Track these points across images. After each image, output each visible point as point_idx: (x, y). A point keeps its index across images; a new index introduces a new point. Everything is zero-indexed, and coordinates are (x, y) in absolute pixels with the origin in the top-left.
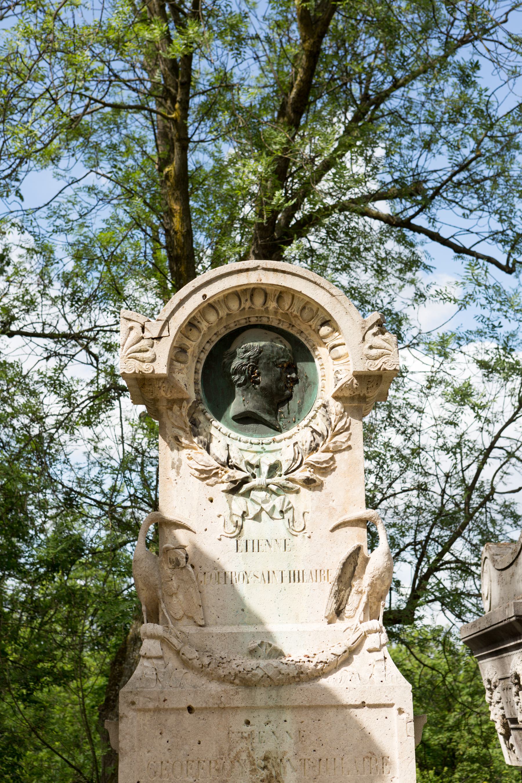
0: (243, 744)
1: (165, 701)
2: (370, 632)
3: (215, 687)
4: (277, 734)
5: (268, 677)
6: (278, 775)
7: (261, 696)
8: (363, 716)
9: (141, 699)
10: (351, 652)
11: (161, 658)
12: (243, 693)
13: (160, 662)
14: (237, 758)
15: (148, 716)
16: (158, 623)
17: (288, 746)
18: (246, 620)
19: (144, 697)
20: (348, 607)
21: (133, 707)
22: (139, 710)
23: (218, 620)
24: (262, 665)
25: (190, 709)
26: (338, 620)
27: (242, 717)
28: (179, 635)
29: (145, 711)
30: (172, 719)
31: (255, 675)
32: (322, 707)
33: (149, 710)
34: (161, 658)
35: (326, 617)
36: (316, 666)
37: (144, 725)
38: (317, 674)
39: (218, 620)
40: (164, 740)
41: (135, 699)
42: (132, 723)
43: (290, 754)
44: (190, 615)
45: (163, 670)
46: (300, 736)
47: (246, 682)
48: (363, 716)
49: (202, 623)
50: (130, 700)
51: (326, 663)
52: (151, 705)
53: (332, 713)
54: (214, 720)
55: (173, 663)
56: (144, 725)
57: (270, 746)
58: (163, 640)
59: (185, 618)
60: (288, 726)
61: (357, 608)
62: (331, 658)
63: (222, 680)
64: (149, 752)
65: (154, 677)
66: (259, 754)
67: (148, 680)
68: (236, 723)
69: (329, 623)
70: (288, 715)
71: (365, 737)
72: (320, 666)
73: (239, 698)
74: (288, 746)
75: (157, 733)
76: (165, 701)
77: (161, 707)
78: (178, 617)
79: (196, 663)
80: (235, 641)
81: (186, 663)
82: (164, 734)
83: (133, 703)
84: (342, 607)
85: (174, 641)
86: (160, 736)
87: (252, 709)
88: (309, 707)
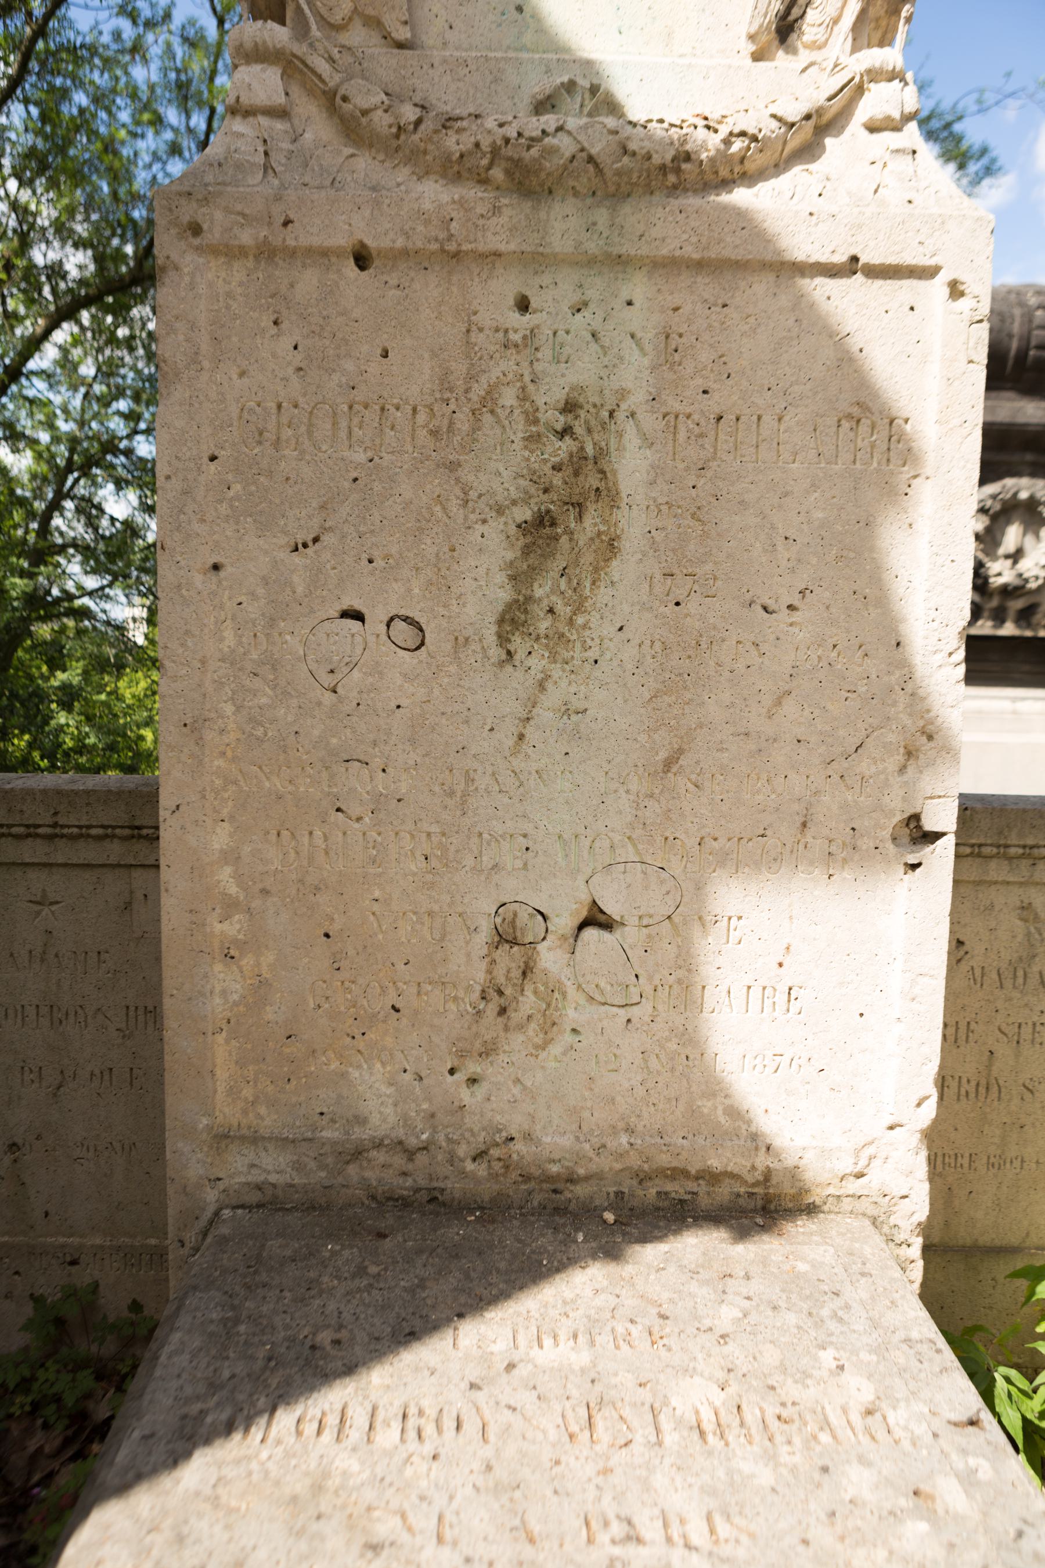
0: (507, 365)
1: (286, 223)
2: (874, 75)
3: (433, 193)
4: (605, 343)
5: (591, 159)
6: (602, 453)
7: (564, 224)
8: (844, 302)
9: (218, 215)
10: (820, 126)
11: (281, 113)
12: (513, 210)
13: (279, 126)
14: (489, 401)
15: (238, 272)
16: (282, 22)
17: (635, 374)
18: (528, 38)
19: (227, 210)
20: (811, 15)
21: (196, 241)
22: (214, 251)
23: (449, 35)
24: (575, 128)
25: (362, 259)
26: (781, 53)
27: (507, 285)
28: (337, 56)
29: (231, 253)
30: (308, 282)
31: (553, 151)
32: (740, 266)
33: (242, 252)
34: (281, 113)
35: (752, 37)
36: (727, 142)
37: (229, 295)
38: (724, 173)
39: (449, 35)
40: (286, 343)
41: (202, 214)
42: (192, 286)
43: (637, 399)
44: (370, 11)
45: (286, 145)
46: (670, 349)
47: (523, 174)
48: (844, 302)
49: (403, 34)
50: (186, 219)
51: (754, 139)
52: (246, 237)
53: (761, 286)
54: (428, 288)
55: (317, 129)
56: (229, 295)
57: (582, 371)
58: (292, 66)
59: (357, 23)
60: (634, 319)
61: (836, 21)
62: (770, 128)
63: (456, 169)
64: (242, 374)
65: (260, 159)
66: (550, 396)
67: (239, 166)
68: (492, 298)
69: (758, 57)
70: (638, 287)
71: (846, 363)
72: (738, 145)
73: (503, 224)
74: (635, 374)
75: (266, 321)
76: (286, 223)
77: (277, 242)
78: (337, 18)
79: (381, 121)
80: (495, 80)
81: (353, 128)
82: (284, 326)
83: (196, 229)
84: (795, 12)
85: (322, 67)
86: (274, 330)
87: (537, 260)
88: (700, 266)
